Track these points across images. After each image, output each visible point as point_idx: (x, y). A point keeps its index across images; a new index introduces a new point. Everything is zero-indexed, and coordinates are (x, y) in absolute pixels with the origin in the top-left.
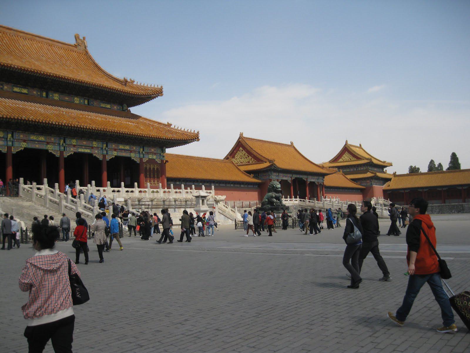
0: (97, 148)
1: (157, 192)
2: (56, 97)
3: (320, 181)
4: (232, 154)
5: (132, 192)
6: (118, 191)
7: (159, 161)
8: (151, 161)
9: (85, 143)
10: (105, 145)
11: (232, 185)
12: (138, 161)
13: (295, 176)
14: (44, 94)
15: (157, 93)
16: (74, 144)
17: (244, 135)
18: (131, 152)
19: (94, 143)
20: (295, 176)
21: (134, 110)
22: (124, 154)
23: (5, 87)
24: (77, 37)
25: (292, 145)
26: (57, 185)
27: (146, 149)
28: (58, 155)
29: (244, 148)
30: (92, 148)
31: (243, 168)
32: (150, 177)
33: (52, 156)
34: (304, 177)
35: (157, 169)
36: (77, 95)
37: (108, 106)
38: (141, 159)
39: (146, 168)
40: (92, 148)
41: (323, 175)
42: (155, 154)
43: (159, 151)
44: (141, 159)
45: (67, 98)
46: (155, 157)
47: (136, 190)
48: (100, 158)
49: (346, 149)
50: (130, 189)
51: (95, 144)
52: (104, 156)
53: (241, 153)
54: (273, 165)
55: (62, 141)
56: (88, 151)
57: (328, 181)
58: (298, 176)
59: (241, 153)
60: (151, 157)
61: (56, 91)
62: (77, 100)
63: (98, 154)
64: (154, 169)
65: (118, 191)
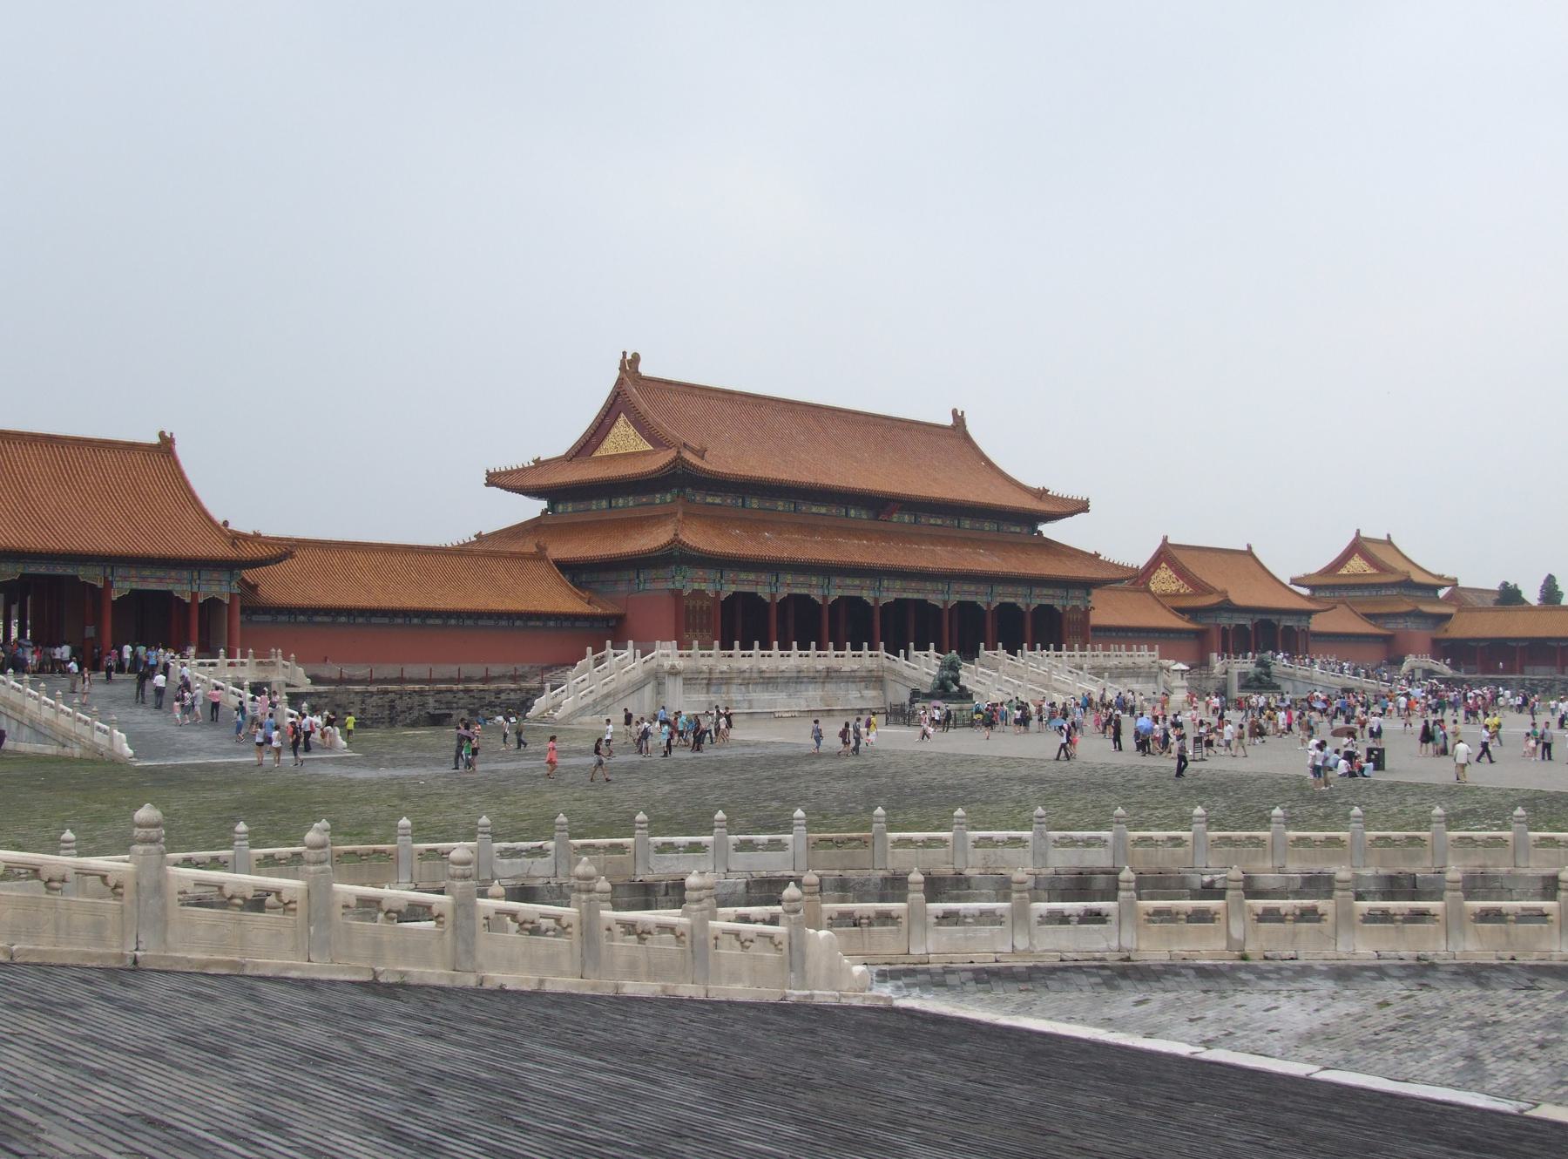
3: (1303, 624)
8: (1075, 608)
13: (1259, 617)
15: (1083, 507)
17: (1170, 541)
20: (1259, 617)
21: (1049, 530)
24: (955, 412)
25: (1249, 553)
34: (1274, 618)
41: (1309, 614)
44: (1064, 607)
49: (1358, 546)
54: (1228, 601)
57: (1318, 624)
58: (1264, 617)
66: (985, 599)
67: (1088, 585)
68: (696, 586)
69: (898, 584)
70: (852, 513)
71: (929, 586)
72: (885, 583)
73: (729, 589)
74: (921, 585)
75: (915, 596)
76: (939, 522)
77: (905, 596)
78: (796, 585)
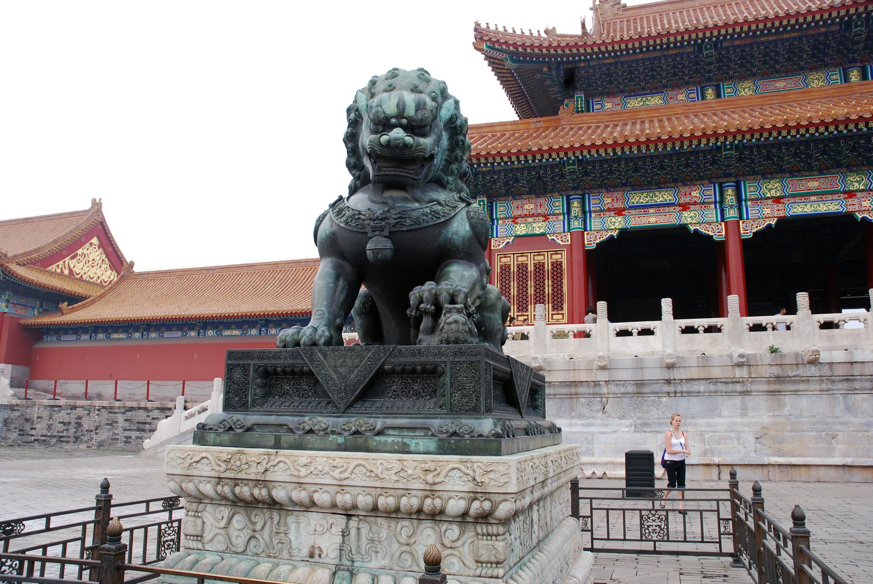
68: (521, 229)
73: (604, 226)
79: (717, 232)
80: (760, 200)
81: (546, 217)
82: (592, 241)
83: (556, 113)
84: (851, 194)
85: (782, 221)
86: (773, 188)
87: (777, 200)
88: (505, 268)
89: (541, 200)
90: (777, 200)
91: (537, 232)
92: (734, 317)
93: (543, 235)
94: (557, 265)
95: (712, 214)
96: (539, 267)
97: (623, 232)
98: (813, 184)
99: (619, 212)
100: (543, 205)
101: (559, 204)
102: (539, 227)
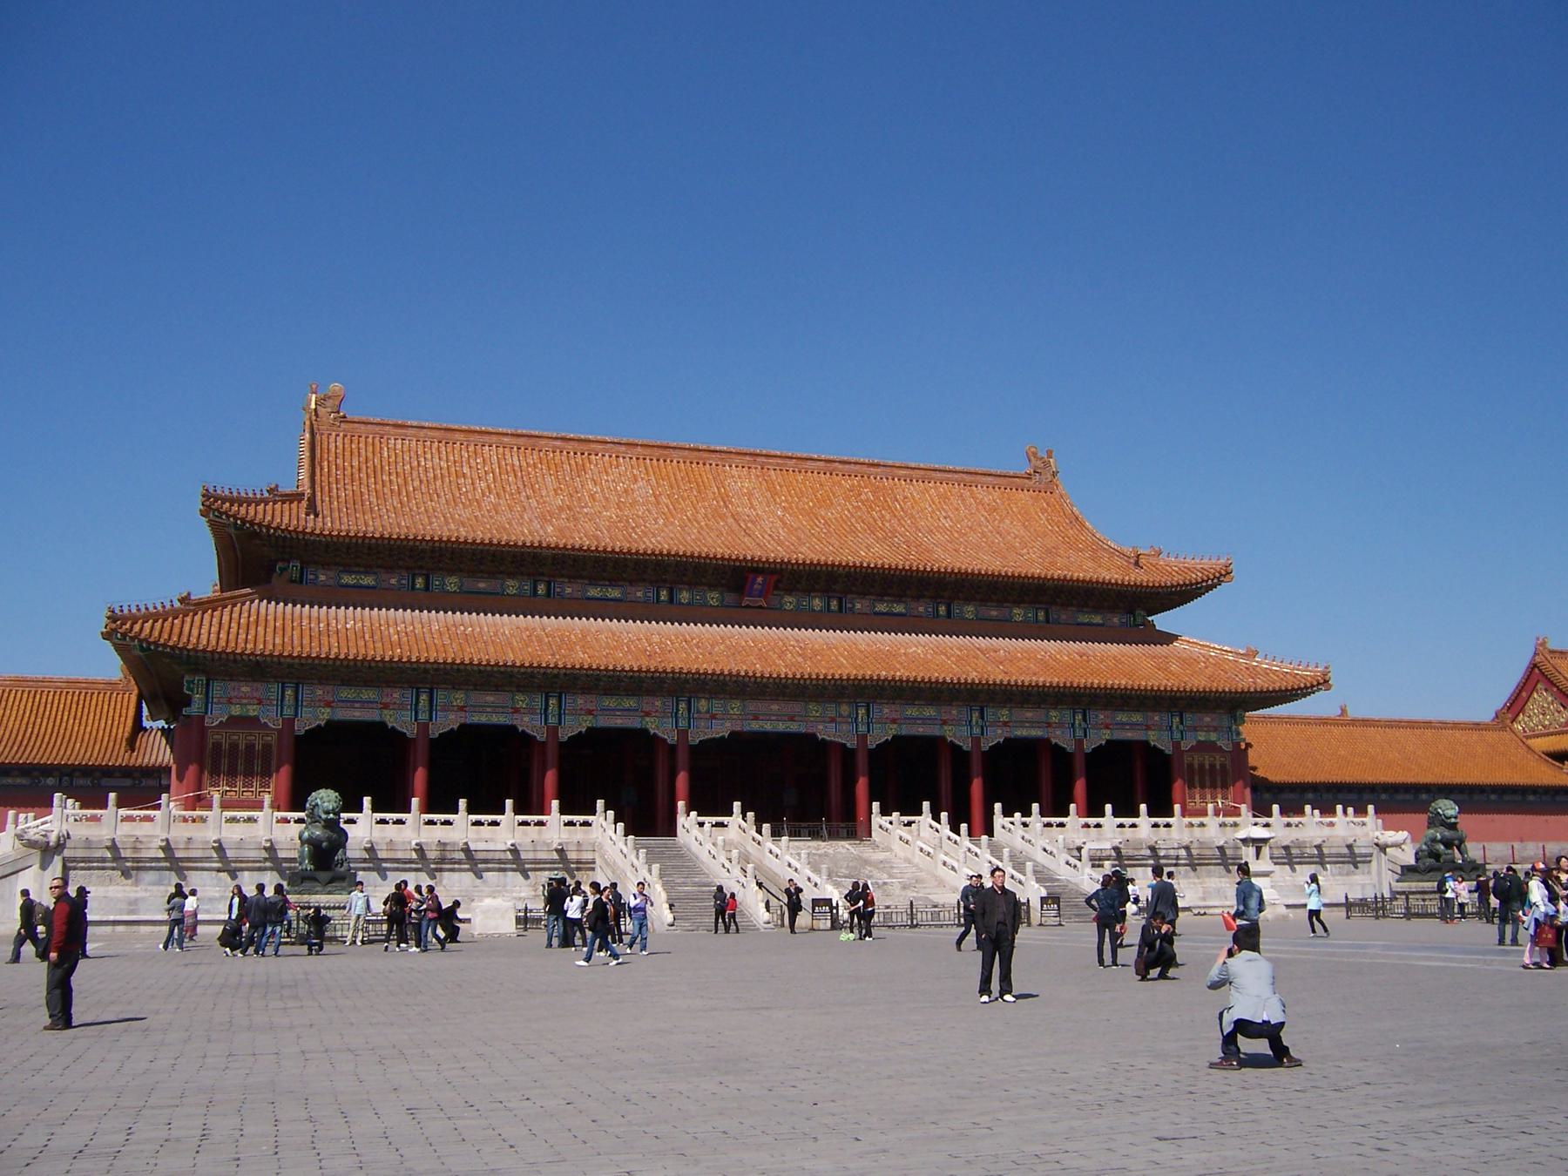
0: (1061, 725)
1: (1202, 825)
2: (969, 611)
4: (1516, 704)
5: (1134, 826)
6: (1098, 826)
7: (1225, 744)
9: (1029, 715)
10: (1080, 717)
11: (1493, 797)
12: (1168, 750)
14: (942, 609)
16: (1005, 719)
18: (1148, 728)
19: (1053, 713)
21: (1162, 621)
22: (1129, 735)
23: (858, 606)
24: (1031, 456)
26: (944, 815)
27: (1189, 718)
28: (967, 746)
29: (1551, 683)
30: (1049, 725)
31: (1541, 744)
32: (1203, 787)
33: (955, 748)
35: (1223, 766)
36: (1017, 603)
37: (1098, 619)
38: (1176, 745)
39: (1190, 766)
40: (1049, 725)
42: (1215, 729)
43: (1225, 720)
44: (1176, 745)
45: (994, 613)
46: (1213, 737)
47: (1144, 820)
48: (1069, 746)
50: (1128, 821)
51: (1054, 715)
52: (1079, 743)
53: (1541, 698)
55: (976, 715)
56: (1035, 733)
59: (1541, 698)
60: (1202, 736)
61: (968, 600)
62: (1018, 613)
63: (1062, 738)
64: (1212, 766)
65: (1098, 826)
66: (964, 731)
67: (1235, 704)
68: (236, 711)
69: (735, 707)
70: (685, 596)
71: (814, 709)
72: (703, 704)
73: (313, 717)
74: (796, 707)
75: (781, 727)
76: (899, 608)
77: (755, 726)
78: (481, 709)
79: (410, 731)
80: (447, 708)
81: (260, 702)
82: (301, 728)
83: (268, 581)
84: (516, 711)
85: (462, 726)
86: (459, 698)
87: (461, 709)
88: (217, 746)
89: (258, 685)
90: (461, 709)
91: (252, 714)
92: (414, 815)
93: (256, 719)
94: (267, 747)
95: (407, 716)
96: (250, 747)
97: (329, 723)
98: (490, 699)
99: (328, 704)
100: (260, 689)
101: (275, 688)
102: (253, 711)
